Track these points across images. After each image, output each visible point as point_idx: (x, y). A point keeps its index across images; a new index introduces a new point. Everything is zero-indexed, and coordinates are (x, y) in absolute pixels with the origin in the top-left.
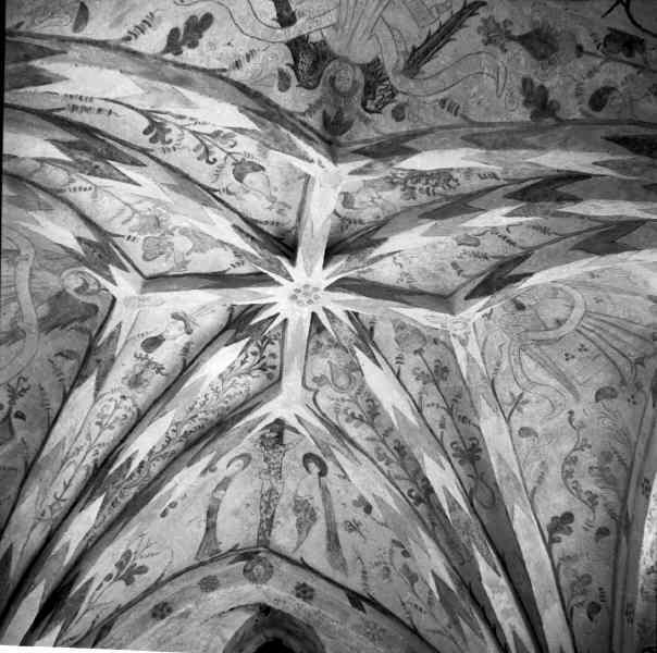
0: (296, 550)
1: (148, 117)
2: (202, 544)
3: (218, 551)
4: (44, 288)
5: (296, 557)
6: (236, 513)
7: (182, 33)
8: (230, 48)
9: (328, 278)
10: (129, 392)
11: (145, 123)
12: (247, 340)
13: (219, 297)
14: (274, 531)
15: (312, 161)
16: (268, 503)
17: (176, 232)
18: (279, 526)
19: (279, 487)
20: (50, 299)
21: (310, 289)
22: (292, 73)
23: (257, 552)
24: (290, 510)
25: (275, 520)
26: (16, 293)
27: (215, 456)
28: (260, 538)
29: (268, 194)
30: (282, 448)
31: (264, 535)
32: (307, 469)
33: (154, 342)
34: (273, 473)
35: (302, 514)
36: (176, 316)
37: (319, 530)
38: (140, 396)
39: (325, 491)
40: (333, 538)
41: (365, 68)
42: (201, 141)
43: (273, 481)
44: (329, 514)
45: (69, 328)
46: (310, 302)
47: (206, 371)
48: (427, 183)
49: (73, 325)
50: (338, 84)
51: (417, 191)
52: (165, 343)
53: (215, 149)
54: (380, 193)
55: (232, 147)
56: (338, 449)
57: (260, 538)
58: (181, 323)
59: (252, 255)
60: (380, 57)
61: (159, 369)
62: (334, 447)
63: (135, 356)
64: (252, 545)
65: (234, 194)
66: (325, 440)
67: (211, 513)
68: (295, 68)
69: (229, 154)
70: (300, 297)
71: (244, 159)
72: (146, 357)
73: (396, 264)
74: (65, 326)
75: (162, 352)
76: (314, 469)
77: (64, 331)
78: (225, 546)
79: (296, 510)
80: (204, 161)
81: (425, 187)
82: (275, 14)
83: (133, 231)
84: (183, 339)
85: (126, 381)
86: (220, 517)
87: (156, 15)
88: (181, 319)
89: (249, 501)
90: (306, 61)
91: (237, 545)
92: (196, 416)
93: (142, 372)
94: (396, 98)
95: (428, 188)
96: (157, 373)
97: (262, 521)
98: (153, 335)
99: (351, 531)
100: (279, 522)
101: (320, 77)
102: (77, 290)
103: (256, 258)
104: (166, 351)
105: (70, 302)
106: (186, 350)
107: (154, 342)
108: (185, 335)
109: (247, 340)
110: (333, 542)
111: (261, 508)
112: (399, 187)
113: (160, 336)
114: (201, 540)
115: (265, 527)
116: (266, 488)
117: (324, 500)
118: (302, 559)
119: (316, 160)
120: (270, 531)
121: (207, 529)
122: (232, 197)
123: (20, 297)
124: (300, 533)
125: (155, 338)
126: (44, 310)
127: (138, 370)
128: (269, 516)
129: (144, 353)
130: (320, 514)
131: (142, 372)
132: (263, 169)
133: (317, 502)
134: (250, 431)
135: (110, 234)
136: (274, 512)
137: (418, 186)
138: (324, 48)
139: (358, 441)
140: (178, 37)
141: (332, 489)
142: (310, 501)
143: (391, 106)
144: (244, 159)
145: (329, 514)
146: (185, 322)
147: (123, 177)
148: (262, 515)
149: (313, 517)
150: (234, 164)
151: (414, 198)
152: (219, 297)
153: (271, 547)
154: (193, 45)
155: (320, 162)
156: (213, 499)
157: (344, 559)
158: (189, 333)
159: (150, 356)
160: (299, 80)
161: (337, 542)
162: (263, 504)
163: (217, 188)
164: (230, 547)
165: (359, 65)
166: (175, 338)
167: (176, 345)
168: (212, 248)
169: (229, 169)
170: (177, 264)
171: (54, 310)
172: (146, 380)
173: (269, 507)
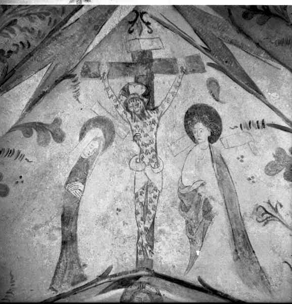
0: (189, 268)
2: (58, 267)
3: (83, 278)
5: (192, 278)
6: (104, 221)
14: (156, 245)
16: (144, 205)
18: (163, 238)
19: (156, 180)
23: (138, 277)
24: (175, 211)
25: (157, 229)
27: (47, 78)
28: (141, 257)
30: (154, 116)
31: (146, 255)
32: (193, 138)
34: (146, 160)
35: (192, 213)
37: (219, 228)
39: (220, 163)
40: (239, 239)
43: (148, 169)
44: (230, 202)
56: (241, 47)
57: (141, 257)
62: (231, 42)
64: (130, 269)
66: (217, 33)
67: (68, 218)
76: (202, 131)
78: (91, 273)
79: (184, 209)
86: (81, 226)
89: (119, 205)
91: (110, 269)
92: (13, 22)
97: (140, 234)
99: (266, 222)
100: (161, 232)
110: (242, 245)
111: (137, 213)
114: (56, 260)
115: (145, 242)
116: (140, 184)
117: (220, 182)
118: (200, 280)
120: (152, 247)
121: (64, 243)
124: (192, 241)
128: (148, 226)
130: (218, 207)
133: (212, 190)
134: (97, 29)
136: (155, 215)
139: (268, 46)
141: (230, 157)
142: (200, 190)
145: (230, 202)
148: (138, 225)
149: (208, 213)
153: (157, 270)
156: (67, 194)
157: (261, 270)
161: (247, 244)
162: (139, 207)
164: (100, 272)
173: (147, 211)
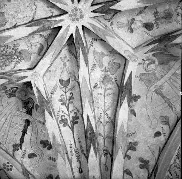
1: (73, 127)
4: (164, 69)
7: (48, 146)
8: (42, 130)
9: (63, 20)
10: (175, 14)
11: (75, 126)
12: (111, 8)
13: (107, 37)
15: (37, 88)
17: (103, 68)
20: (166, 64)
21: (73, 17)
22: (34, 107)
26: (173, 75)
29: (65, 68)
33: (148, 26)
36: (132, 31)
38: (172, 8)
41: (14, 96)
42: (69, 104)
45: (170, 53)
46: (76, 10)
47: (136, 4)
48: (6, 52)
49: (167, 53)
50: (25, 94)
51: (12, 47)
52: (145, 22)
53: (68, 98)
54: (27, 49)
55: (63, 95)
58: (133, 26)
59: (82, 51)
60: (8, 98)
61: (156, 13)
63: (158, 28)
65: (74, 76)
68: (33, 107)
69: (66, 93)
70: (79, 14)
71: (63, 87)
72: (156, 23)
73: (36, 5)
74: (171, 54)
75: (149, 20)
77: (172, 53)
80: (73, 96)
81: (8, 50)
82: (29, 127)
83: (113, 82)
84: (138, 18)
85: (171, 21)
87: (48, 157)
88: (131, 28)
90: (30, 106)
93: (163, 18)
94: (4, 91)
95: (7, 49)
96: (158, 12)
98: (146, 30)
101: (28, 99)
102: (154, 63)
103: (82, 48)
104: (148, 19)
105: (161, 60)
106: (140, 13)
107: (148, 26)
108: (136, 19)
109: (111, 8)
112: (18, 51)
113: (143, 27)
119: (36, 87)
122: (75, 75)
123: (174, 72)
125: (146, 28)
126: (172, 63)
127: (163, 20)
129: (155, 25)
131: (163, 18)
132: (60, 80)
135: (118, 88)
137: (10, 51)
138: (24, 105)
140: (48, 147)
143: (7, 89)
144: (63, 87)
146: (131, 26)
147: (88, 123)
150: (67, 87)
151: (14, 44)
152: (107, 37)
154: (47, 141)
155: (35, 86)
158: (134, 19)
159: (154, 22)
160: (34, 104)
163: (77, 83)
165: (16, 97)
166: (140, 21)
167: (142, 18)
168: (98, 53)
169: (69, 87)
170: (114, 54)
171: (168, 61)
172: (165, 13)
